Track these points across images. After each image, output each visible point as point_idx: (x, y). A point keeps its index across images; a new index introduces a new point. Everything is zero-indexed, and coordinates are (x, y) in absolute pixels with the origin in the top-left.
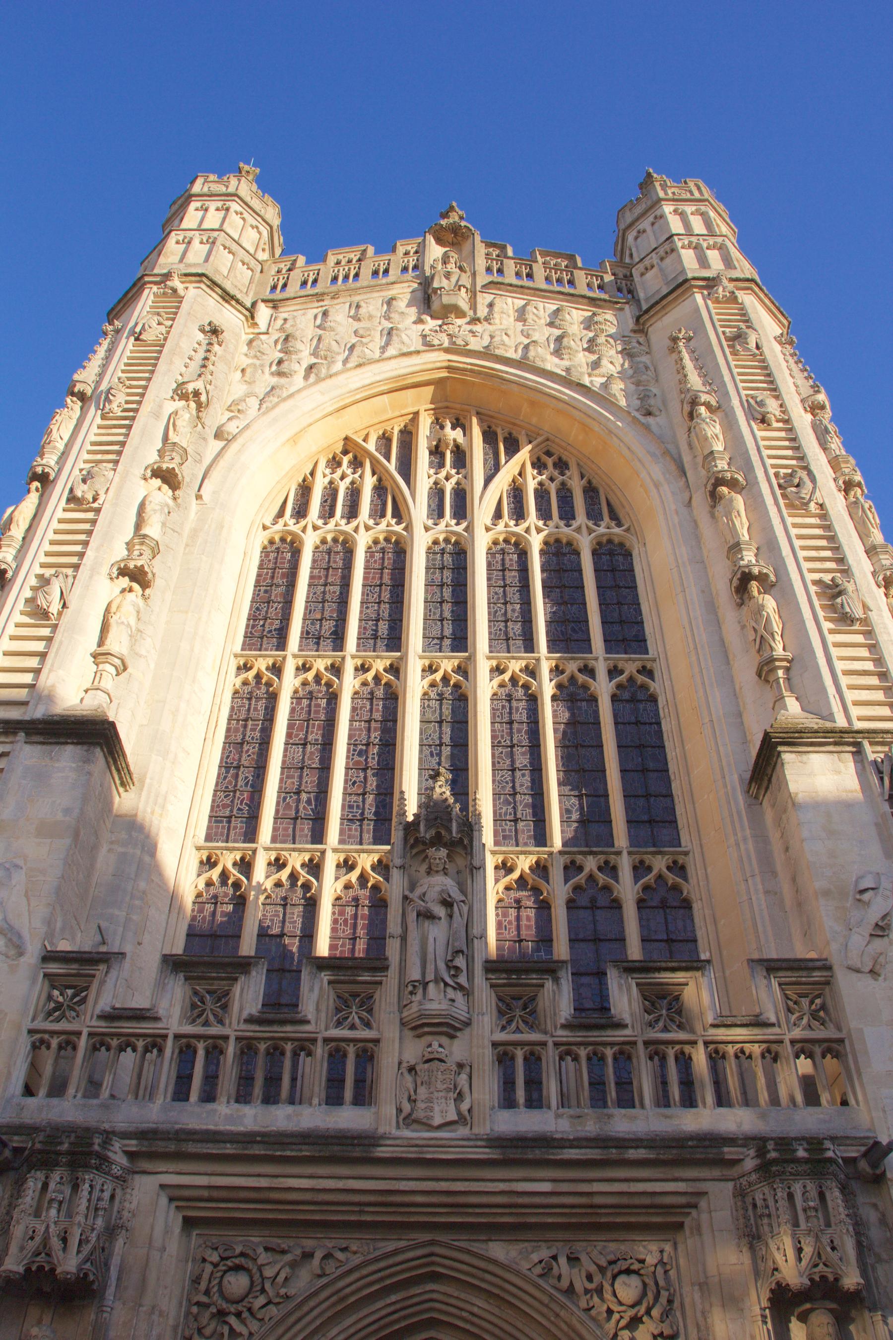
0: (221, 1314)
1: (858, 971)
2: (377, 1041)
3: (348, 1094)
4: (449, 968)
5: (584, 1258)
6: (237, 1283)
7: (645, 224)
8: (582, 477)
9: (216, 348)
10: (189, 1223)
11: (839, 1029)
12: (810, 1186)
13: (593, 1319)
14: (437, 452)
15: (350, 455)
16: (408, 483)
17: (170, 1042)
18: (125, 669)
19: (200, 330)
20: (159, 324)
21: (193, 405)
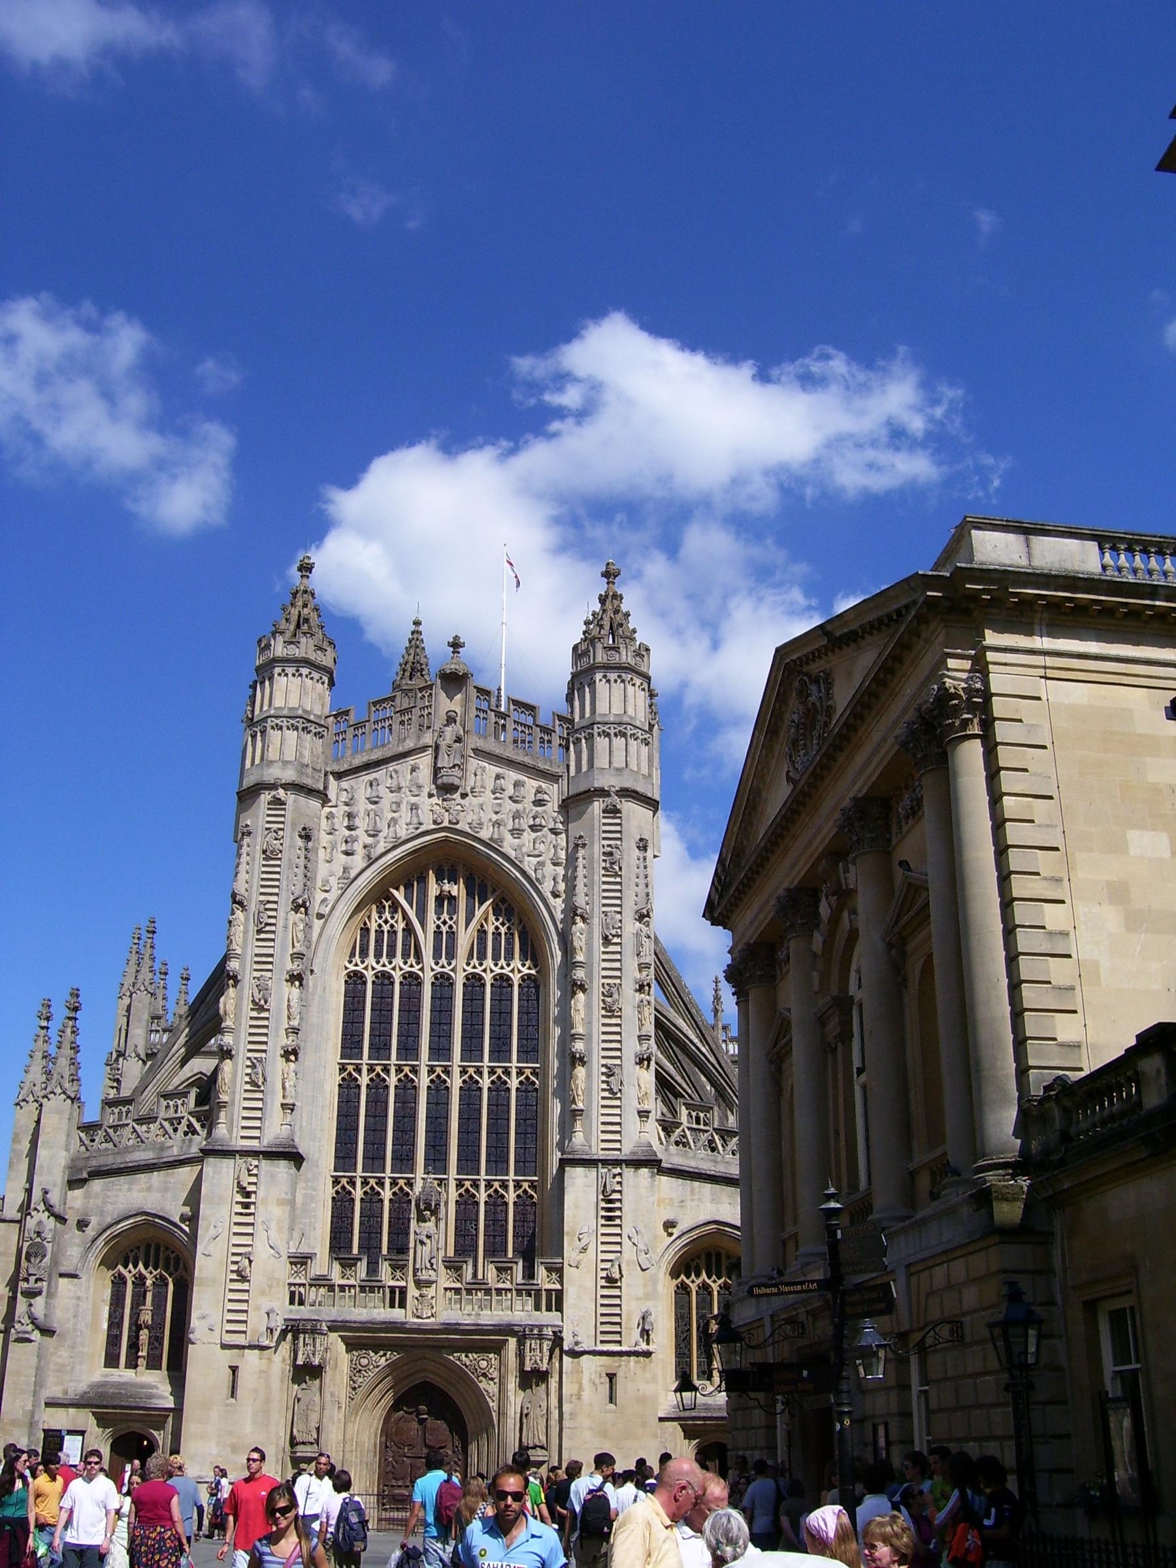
0: (360, 1371)
1: (571, 1266)
2: (406, 1287)
3: (397, 1305)
4: (430, 1261)
5: (470, 1355)
6: (364, 1362)
7: (586, 680)
8: (521, 921)
9: (310, 844)
10: (347, 1344)
11: (562, 1285)
12: (538, 1341)
13: (473, 1373)
14: (440, 899)
15: (390, 902)
16: (423, 924)
17: (336, 1287)
18: (294, 1105)
19: (300, 836)
20: (276, 839)
21: (303, 909)
